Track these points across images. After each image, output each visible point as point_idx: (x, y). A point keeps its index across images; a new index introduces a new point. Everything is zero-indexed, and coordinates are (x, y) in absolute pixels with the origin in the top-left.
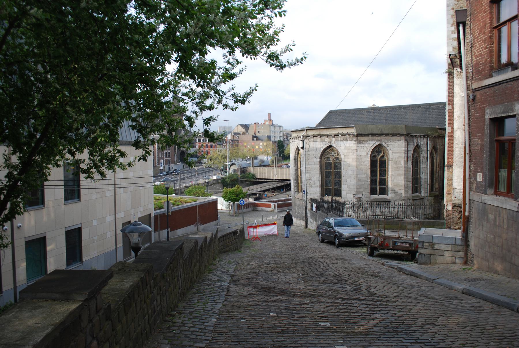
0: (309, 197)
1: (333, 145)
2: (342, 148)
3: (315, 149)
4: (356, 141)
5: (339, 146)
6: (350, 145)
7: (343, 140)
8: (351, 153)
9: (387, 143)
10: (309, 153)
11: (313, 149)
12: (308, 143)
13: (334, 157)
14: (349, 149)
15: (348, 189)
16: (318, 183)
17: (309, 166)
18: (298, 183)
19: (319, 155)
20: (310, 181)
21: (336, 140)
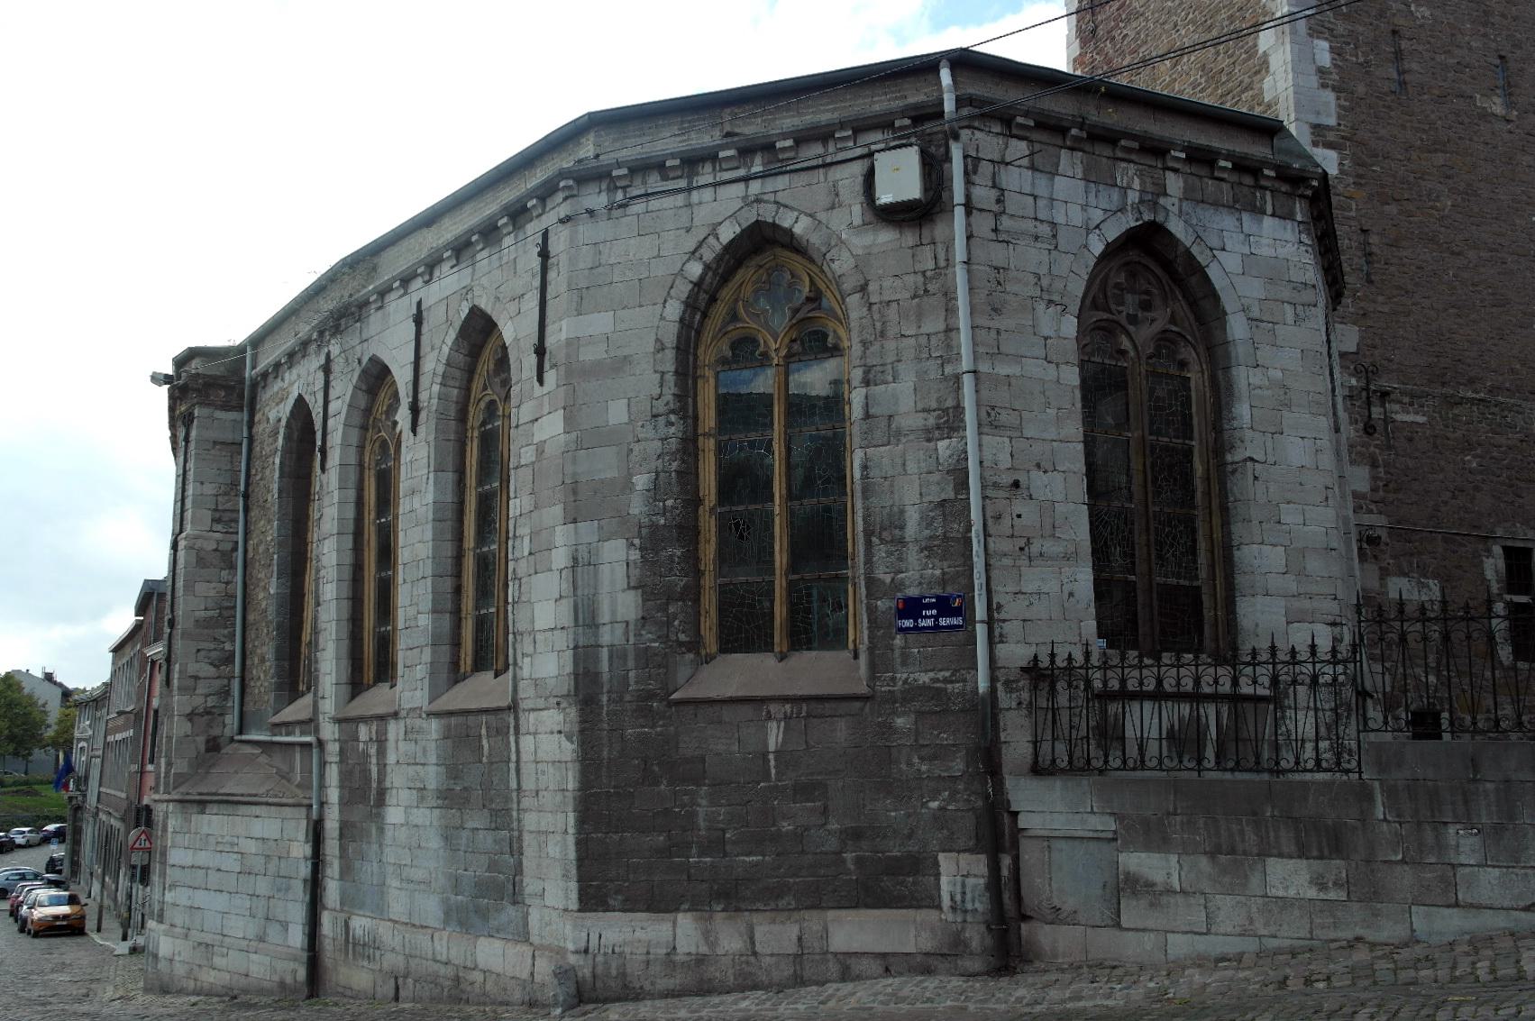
0: (1015, 653)
1: (1176, 227)
2: (1231, 261)
3: (1045, 230)
5: (1214, 241)
8: (1288, 309)
10: (998, 254)
11: (1029, 225)
12: (986, 169)
14: (1273, 274)
15: (1291, 584)
17: (1003, 370)
19: (1078, 287)
20: (1019, 506)
21: (1188, 196)
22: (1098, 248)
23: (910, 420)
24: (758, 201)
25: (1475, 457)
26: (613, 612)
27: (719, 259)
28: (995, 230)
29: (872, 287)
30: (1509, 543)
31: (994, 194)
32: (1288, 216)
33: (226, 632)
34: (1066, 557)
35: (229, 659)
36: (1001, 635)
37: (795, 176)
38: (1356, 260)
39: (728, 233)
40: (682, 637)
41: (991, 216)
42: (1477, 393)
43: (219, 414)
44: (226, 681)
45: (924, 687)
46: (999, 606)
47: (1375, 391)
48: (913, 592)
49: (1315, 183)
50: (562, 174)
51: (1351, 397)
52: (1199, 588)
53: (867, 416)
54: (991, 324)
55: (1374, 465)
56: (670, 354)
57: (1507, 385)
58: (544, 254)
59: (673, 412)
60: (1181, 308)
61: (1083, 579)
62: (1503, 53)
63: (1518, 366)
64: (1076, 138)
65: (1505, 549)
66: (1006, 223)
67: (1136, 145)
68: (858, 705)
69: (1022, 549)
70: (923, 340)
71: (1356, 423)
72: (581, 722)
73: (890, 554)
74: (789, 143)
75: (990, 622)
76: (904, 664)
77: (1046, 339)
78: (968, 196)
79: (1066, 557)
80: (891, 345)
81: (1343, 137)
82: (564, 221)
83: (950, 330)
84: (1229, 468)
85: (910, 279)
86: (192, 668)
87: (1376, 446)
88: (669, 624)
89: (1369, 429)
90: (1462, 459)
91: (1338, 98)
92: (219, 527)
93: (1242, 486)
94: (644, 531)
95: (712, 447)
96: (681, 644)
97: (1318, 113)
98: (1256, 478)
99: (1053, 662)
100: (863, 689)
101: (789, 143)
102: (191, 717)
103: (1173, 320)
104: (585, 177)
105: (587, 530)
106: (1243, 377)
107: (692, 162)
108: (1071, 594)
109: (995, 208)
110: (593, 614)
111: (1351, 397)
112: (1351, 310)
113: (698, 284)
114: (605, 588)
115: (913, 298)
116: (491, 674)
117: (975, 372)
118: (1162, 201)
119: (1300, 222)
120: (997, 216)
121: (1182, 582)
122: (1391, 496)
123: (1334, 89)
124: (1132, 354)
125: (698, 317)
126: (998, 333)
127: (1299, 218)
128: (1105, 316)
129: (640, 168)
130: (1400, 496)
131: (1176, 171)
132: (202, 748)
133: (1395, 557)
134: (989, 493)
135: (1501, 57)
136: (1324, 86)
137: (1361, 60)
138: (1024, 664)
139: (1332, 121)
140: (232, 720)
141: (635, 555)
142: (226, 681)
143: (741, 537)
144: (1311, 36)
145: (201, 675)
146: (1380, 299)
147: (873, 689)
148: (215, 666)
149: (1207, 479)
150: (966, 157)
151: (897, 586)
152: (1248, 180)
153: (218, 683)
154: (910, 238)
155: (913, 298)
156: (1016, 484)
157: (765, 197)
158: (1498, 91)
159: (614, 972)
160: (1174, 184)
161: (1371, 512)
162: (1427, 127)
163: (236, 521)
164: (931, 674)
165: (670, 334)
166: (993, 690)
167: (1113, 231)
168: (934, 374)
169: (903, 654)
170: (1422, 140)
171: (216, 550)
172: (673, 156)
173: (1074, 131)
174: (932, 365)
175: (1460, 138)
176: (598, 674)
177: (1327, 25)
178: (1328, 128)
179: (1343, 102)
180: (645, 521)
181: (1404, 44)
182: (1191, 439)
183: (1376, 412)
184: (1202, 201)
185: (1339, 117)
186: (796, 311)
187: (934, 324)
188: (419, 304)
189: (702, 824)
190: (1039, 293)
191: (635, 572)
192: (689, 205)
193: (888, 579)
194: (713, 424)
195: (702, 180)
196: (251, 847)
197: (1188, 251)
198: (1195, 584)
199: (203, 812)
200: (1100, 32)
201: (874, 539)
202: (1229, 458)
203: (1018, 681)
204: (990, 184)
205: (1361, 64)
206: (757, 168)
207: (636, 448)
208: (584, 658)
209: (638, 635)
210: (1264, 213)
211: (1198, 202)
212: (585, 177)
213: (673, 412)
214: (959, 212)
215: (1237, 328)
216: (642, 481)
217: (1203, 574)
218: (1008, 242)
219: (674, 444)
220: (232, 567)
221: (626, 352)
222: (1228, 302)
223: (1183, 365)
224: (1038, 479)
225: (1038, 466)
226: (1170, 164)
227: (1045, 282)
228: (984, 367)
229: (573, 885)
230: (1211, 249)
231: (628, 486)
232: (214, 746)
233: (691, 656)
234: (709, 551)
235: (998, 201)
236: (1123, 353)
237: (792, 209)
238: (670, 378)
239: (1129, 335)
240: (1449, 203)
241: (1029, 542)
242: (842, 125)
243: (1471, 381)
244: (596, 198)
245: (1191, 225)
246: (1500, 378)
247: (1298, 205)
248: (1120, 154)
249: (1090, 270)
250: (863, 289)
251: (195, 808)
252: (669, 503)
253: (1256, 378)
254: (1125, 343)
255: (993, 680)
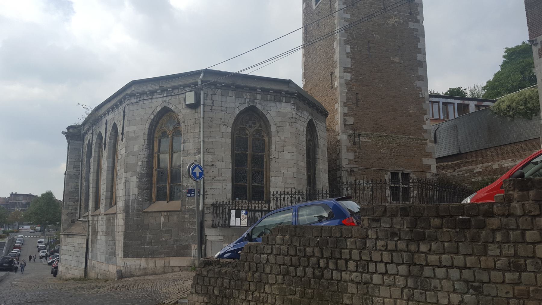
0: (210, 201)
1: (259, 106)
2: (273, 113)
3: (224, 109)
4: (294, 104)
5: (268, 109)
6: (287, 111)
7: (275, 101)
8: (288, 123)
9: (317, 122)
10: (211, 115)
11: (220, 108)
12: (210, 96)
13: (253, 130)
15: (283, 185)
16: (229, 174)
17: (211, 140)
18: (152, 184)
19: (232, 121)
21: (262, 99)
22: (237, 112)
23: (192, 151)
24: (165, 102)
25: (384, 150)
26: (133, 193)
27: (157, 114)
28: (211, 109)
29: (186, 122)
30: (392, 171)
31: (211, 102)
32: (290, 102)
33: (76, 194)
34: (224, 180)
35: (77, 201)
36: (206, 198)
37: (172, 97)
38: (354, 101)
39: (159, 109)
40: (146, 198)
41: (210, 107)
42: (387, 133)
43: (76, 142)
44: (76, 206)
45: (191, 209)
46: (206, 191)
47: (357, 134)
48: (190, 188)
49: (296, 94)
50: (127, 95)
51: (350, 136)
52: (264, 186)
53: (184, 150)
54: (208, 130)
55: (355, 152)
56: (146, 135)
57: (396, 131)
58: (124, 112)
59: (146, 148)
60: (262, 124)
61: (229, 186)
62: (400, 46)
63: (399, 126)
64: (232, 88)
65: (391, 173)
66: (214, 107)
67: (248, 89)
68: (179, 212)
69: (213, 179)
70: (195, 134)
71: (351, 142)
72: (126, 216)
73: (186, 180)
74: (171, 89)
75: (204, 195)
76: (188, 204)
77: (223, 133)
78: (204, 102)
79: (224, 180)
80: (189, 134)
81: (352, 70)
82: (128, 105)
83: (200, 131)
84: (270, 160)
85: (193, 120)
86: (68, 203)
87: (356, 148)
88: (143, 195)
89: (354, 143)
90: (380, 151)
91: (352, 60)
92: (75, 169)
93: (272, 164)
94: (140, 174)
95: (157, 156)
96: (146, 199)
97: (346, 64)
98: (275, 162)
99: (217, 203)
100: (179, 209)
101: (171, 89)
102: (68, 214)
103: (260, 126)
104: (132, 95)
105: (129, 174)
106: (273, 139)
107: (152, 93)
108: (225, 188)
109: (212, 105)
110: (129, 193)
111: (350, 136)
112: (352, 114)
113: (153, 120)
114: (131, 187)
115: (194, 124)
116: (166, 202)
117: (203, 141)
118: (255, 101)
119: (292, 104)
120: (211, 106)
121: (259, 185)
122: (360, 160)
123: (351, 58)
124: (249, 135)
125: (153, 127)
126: (210, 132)
127: (292, 102)
128: (242, 126)
129: (142, 94)
130: (362, 160)
131: (259, 94)
132: (70, 222)
133: (360, 175)
134: (205, 167)
135: (399, 47)
136: (348, 57)
137: (359, 50)
138: (212, 204)
139: (349, 66)
140: (78, 215)
141: (138, 180)
142: (76, 206)
143: (162, 175)
144: (345, 44)
145: (70, 204)
146: (360, 110)
147: (182, 209)
148: (74, 202)
149: (266, 162)
150: (204, 94)
151: (187, 187)
152: (279, 95)
153: (74, 207)
154: (194, 111)
155: (194, 124)
156: (213, 165)
157: (166, 101)
158: (398, 56)
159: (129, 271)
160: (259, 97)
161: (354, 164)
162: (376, 66)
163: (79, 168)
164: (193, 206)
165: (147, 131)
166: (203, 210)
167: (242, 108)
168: (196, 141)
169: (188, 202)
170: (375, 70)
171: (74, 175)
172: (148, 91)
173: (232, 87)
174: (196, 139)
175: (386, 69)
176: (129, 206)
177: (350, 41)
178: (349, 68)
179: (353, 61)
180: (140, 172)
181: (371, 45)
182: (264, 153)
183: (357, 139)
184: (266, 100)
185: (351, 65)
186: (174, 126)
187: (197, 130)
188: (107, 120)
189: (148, 239)
190: (221, 123)
191: (137, 184)
192: (152, 102)
193: (186, 185)
194: (157, 151)
195: (154, 97)
196: (76, 245)
197: (261, 111)
198: (263, 185)
199: (68, 237)
200: (308, 39)
201: (184, 177)
202: (271, 157)
203: (209, 207)
204: (210, 99)
205: (359, 51)
206: (165, 95)
207: (139, 156)
208: (127, 202)
209: (137, 197)
210: (282, 101)
211: (265, 100)
212: (132, 95)
213: (146, 148)
214: (202, 106)
215: (273, 128)
216: (140, 163)
217: (265, 183)
218: (214, 112)
219: (146, 156)
220: (78, 179)
221: (138, 135)
222: (271, 123)
223: (263, 136)
224: (218, 163)
225: (219, 161)
226: (257, 92)
227: (223, 120)
228: (206, 140)
229: (123, 252)
230: (268, 111)
231: (137, 165)
232: (73, 221)
233: (149, 202)
234: (155, 179)
235: (212, 103)
236: (247, 134)
237: (171, 104)
238: (146, 141)
239: (248, 130)
240: (381, 85)
241: (215, 177)
242: (181, 86)
243: (385, 131)
244: (134, 100)
245: (263, 106)
246: (394, 130)
247: (292, 100)
248: (244, 91)
249: (235, 117)
250: (184, 122)
251: (67, 236)
252: (145, 168)
253: (278, 139)
254: (247, 132)
255: (203, 207)
